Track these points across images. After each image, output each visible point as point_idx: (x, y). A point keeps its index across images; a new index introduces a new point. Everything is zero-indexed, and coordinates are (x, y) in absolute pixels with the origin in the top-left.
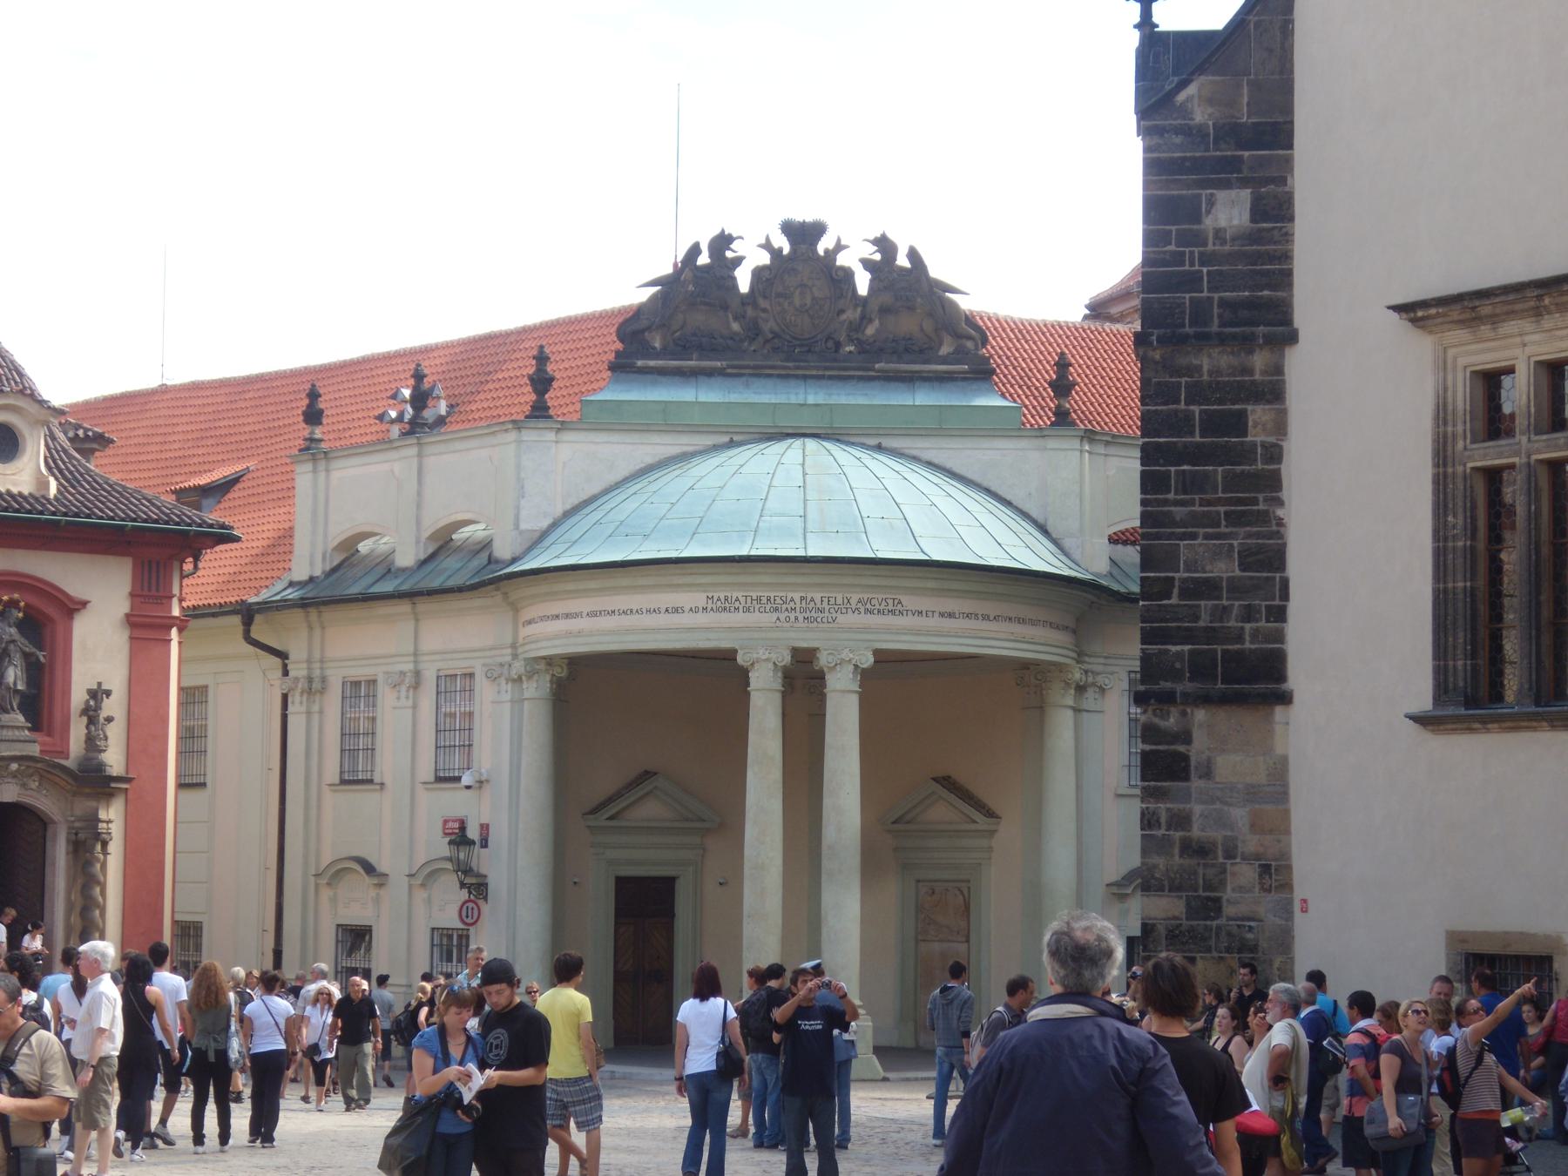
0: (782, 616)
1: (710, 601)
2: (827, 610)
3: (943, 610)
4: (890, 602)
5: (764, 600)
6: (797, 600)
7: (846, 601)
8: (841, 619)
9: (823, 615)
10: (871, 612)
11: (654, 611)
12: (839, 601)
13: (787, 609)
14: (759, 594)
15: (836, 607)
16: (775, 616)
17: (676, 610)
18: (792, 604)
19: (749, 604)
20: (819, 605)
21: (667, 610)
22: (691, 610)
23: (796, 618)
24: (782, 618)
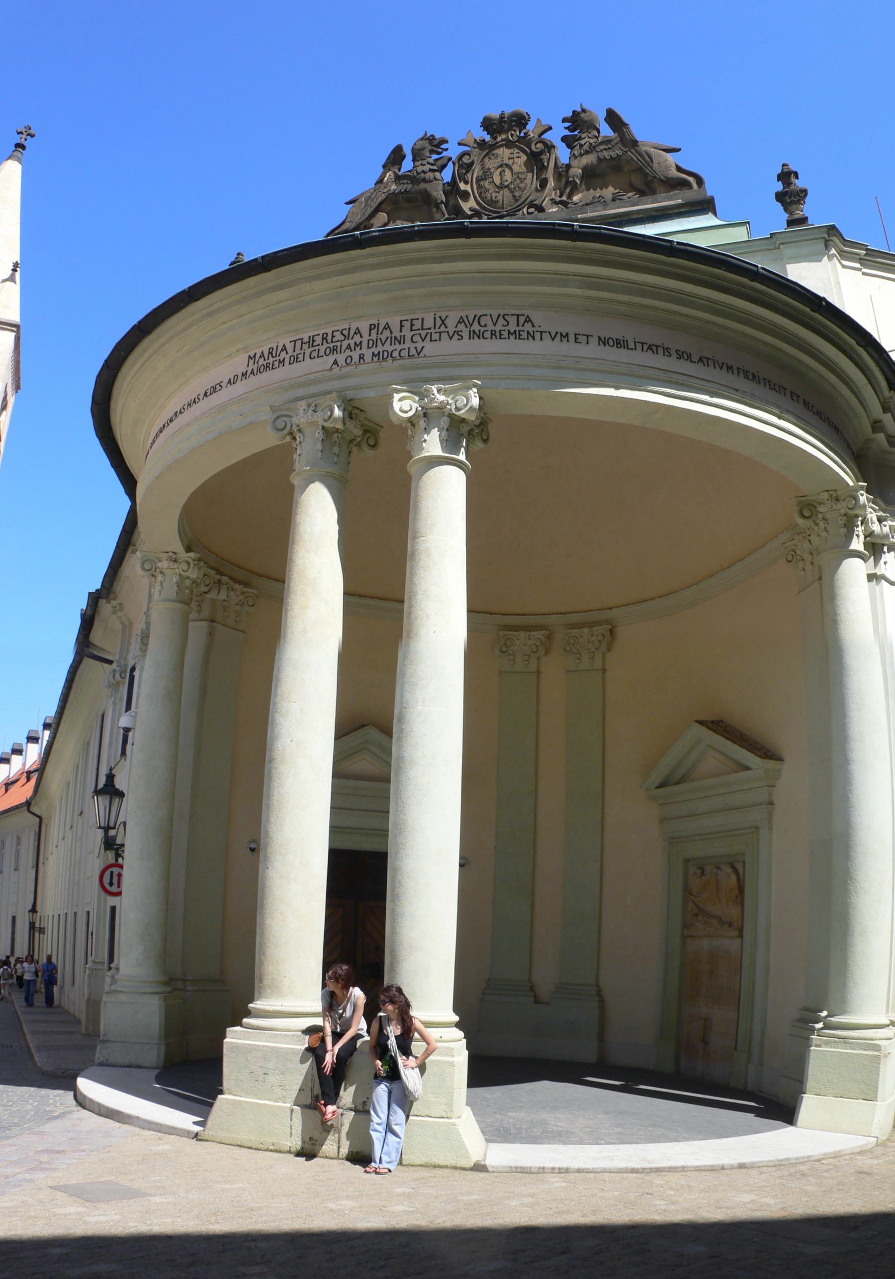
0: (341, 359)
1: (251, 362)
2: (408, 339)
3: (605, 334)
4: (512, 320)
5: (318, 340)
6: (365, 331)
7: (439, 322)
8: (430, 348)
9: (402, 346)
10: (480, 336)
11: (194, 402)
12: (429, 323)
13: (349, 347)
14: (311, 334)
15: (423, 333)
16: (331, 359)
17: (214, 389)
18: (357, 339)
19: (298, 351)
20: (397, 333)
21: (205, 394)
22: (229, 382)
23: (361, 357)
24: (341, 359)
